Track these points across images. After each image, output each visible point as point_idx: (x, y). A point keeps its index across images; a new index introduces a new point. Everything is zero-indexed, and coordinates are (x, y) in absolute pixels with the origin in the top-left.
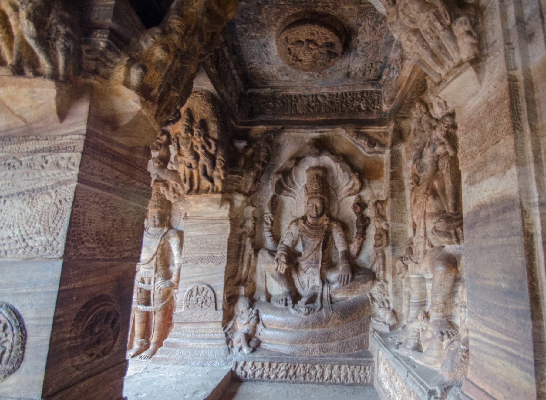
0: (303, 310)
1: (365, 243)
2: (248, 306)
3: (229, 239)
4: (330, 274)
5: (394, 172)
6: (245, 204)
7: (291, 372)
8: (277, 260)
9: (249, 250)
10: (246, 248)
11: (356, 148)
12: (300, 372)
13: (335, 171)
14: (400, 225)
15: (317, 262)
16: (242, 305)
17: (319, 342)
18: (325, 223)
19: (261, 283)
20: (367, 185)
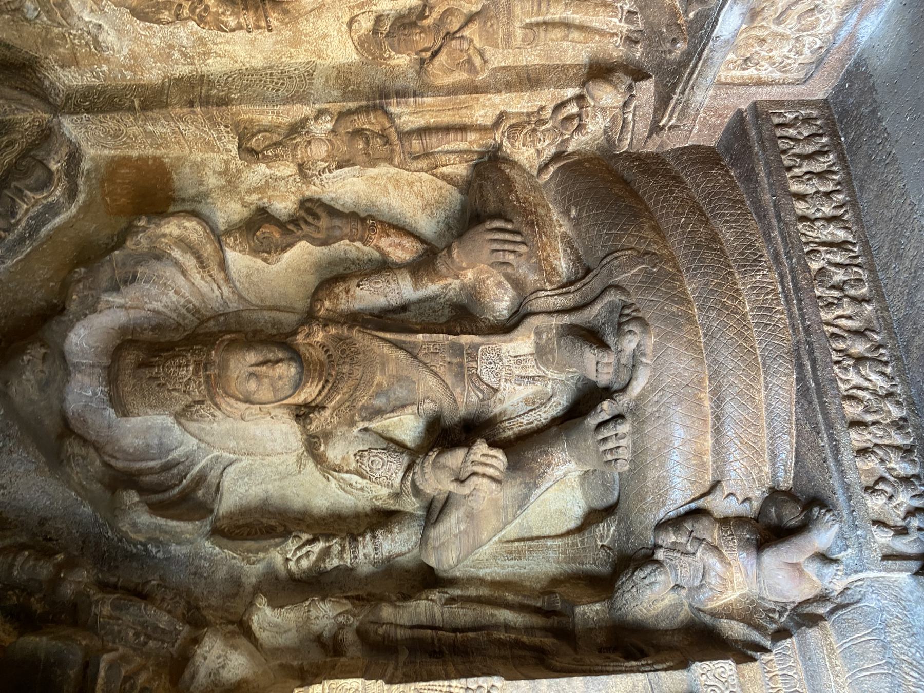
0: (629, 344)
1: (381, 218)
2: (649, 569)
3: (390, 682)
4: (493, 309)
5: (142, 102)
6: (243, 641)
7: (859, 347)
8: (460, 481)
9: (427, 608)
10: (424, 620)
11: (49, 237)
12: (849, 318)
13: (133, 314)
14: (318, 82)
15: (458, 350)
16: (653, 597)
17: (732, 274)
18: (320, 336)
19: (551, 554)
20: (187, 207)
